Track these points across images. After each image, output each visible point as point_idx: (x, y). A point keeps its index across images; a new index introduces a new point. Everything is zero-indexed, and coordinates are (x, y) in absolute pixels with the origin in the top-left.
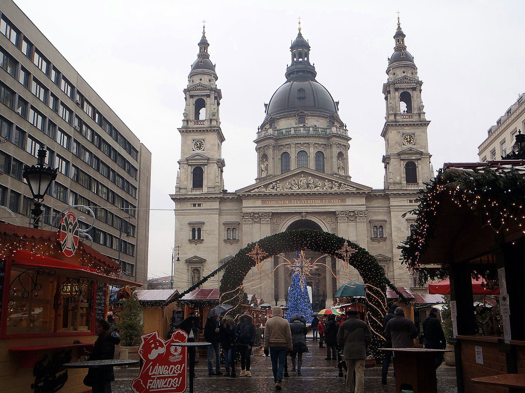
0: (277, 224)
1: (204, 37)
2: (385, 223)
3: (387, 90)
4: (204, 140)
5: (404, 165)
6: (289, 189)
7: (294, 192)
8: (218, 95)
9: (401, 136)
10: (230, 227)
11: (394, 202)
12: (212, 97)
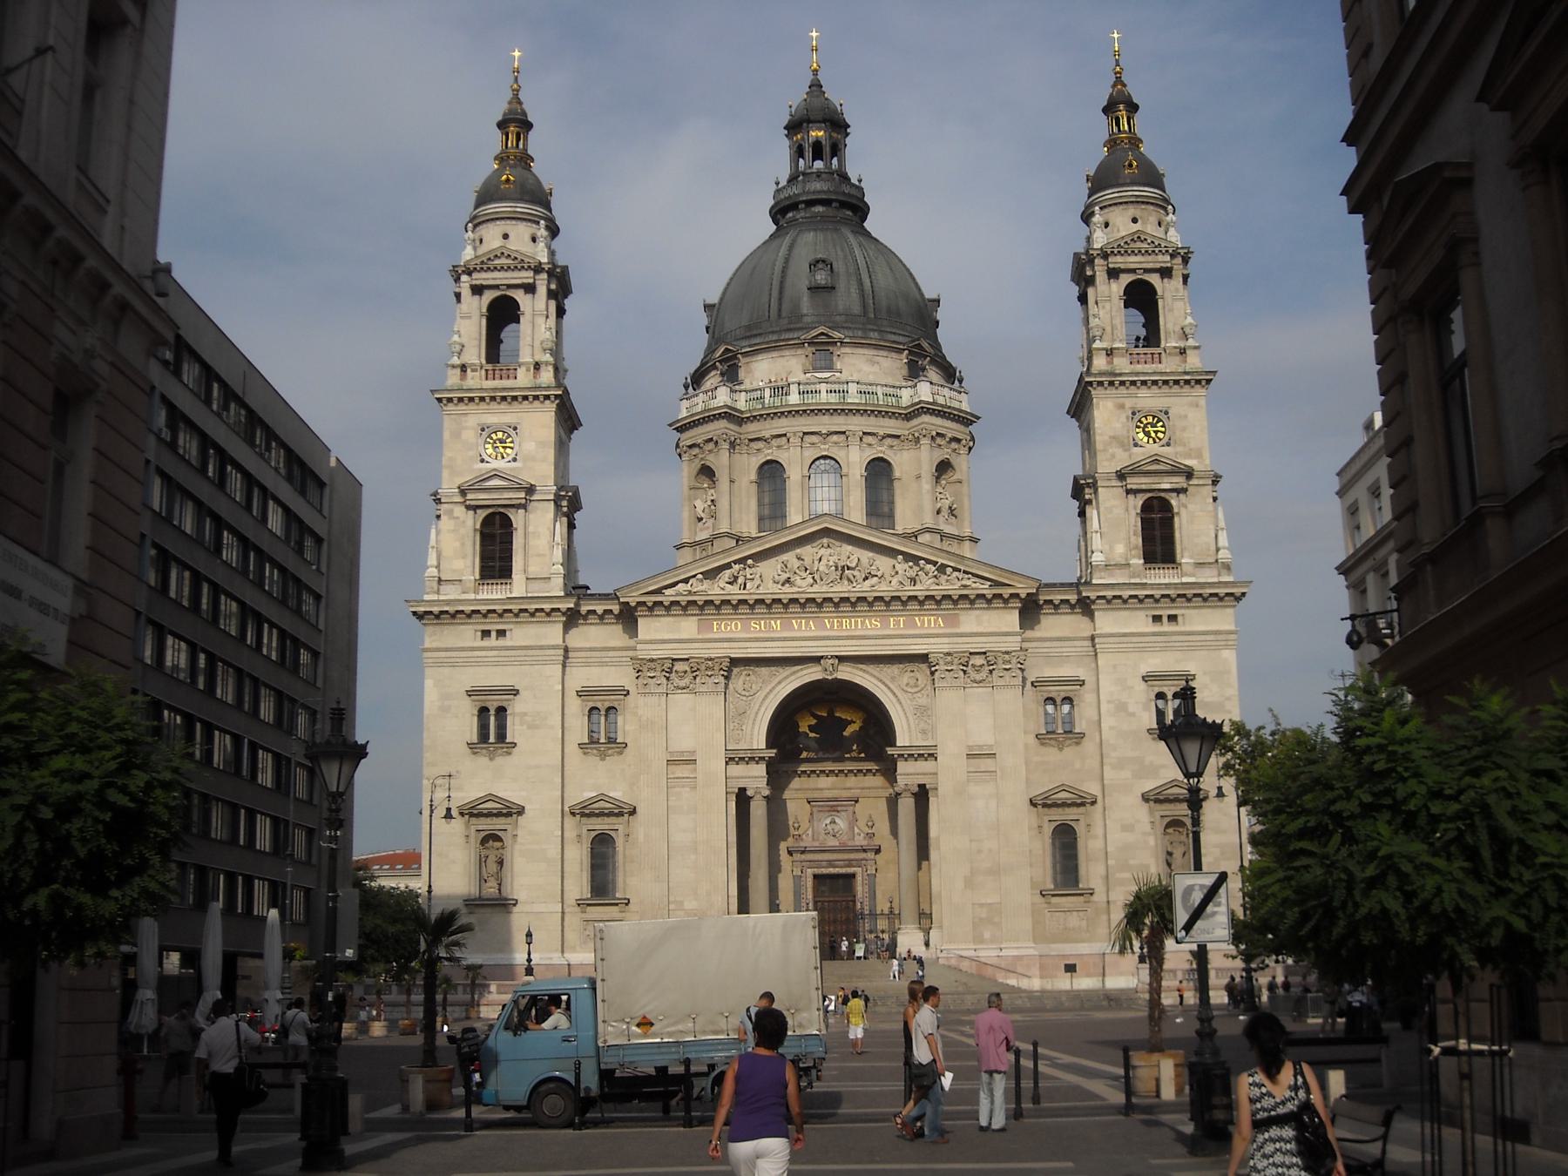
1: (516, 99)
3: (1082, 277)
4: (515, 429)
5: (1135, 508)
6: (783, 585)
7: (798, 593)
8: (561, 288)
9: (1127, 418)
10: (599, 705)
11: (1106, 622)
12: (542, 290)
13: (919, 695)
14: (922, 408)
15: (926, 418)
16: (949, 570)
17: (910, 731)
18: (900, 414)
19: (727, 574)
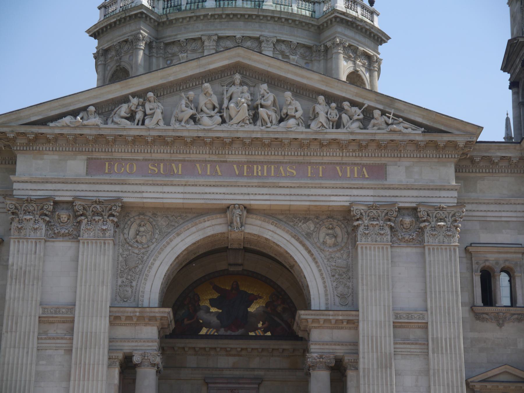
0: (140, 246)
2: (520, 256)
6: (187, 122)
13: (338, 255)
14: (336, 17)
15: (340, 29)
16: (377, 113)
17: (326, 295)
18: (313, 25)
19: (124, 109)
